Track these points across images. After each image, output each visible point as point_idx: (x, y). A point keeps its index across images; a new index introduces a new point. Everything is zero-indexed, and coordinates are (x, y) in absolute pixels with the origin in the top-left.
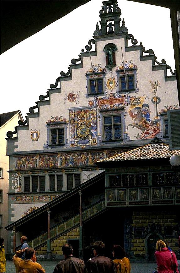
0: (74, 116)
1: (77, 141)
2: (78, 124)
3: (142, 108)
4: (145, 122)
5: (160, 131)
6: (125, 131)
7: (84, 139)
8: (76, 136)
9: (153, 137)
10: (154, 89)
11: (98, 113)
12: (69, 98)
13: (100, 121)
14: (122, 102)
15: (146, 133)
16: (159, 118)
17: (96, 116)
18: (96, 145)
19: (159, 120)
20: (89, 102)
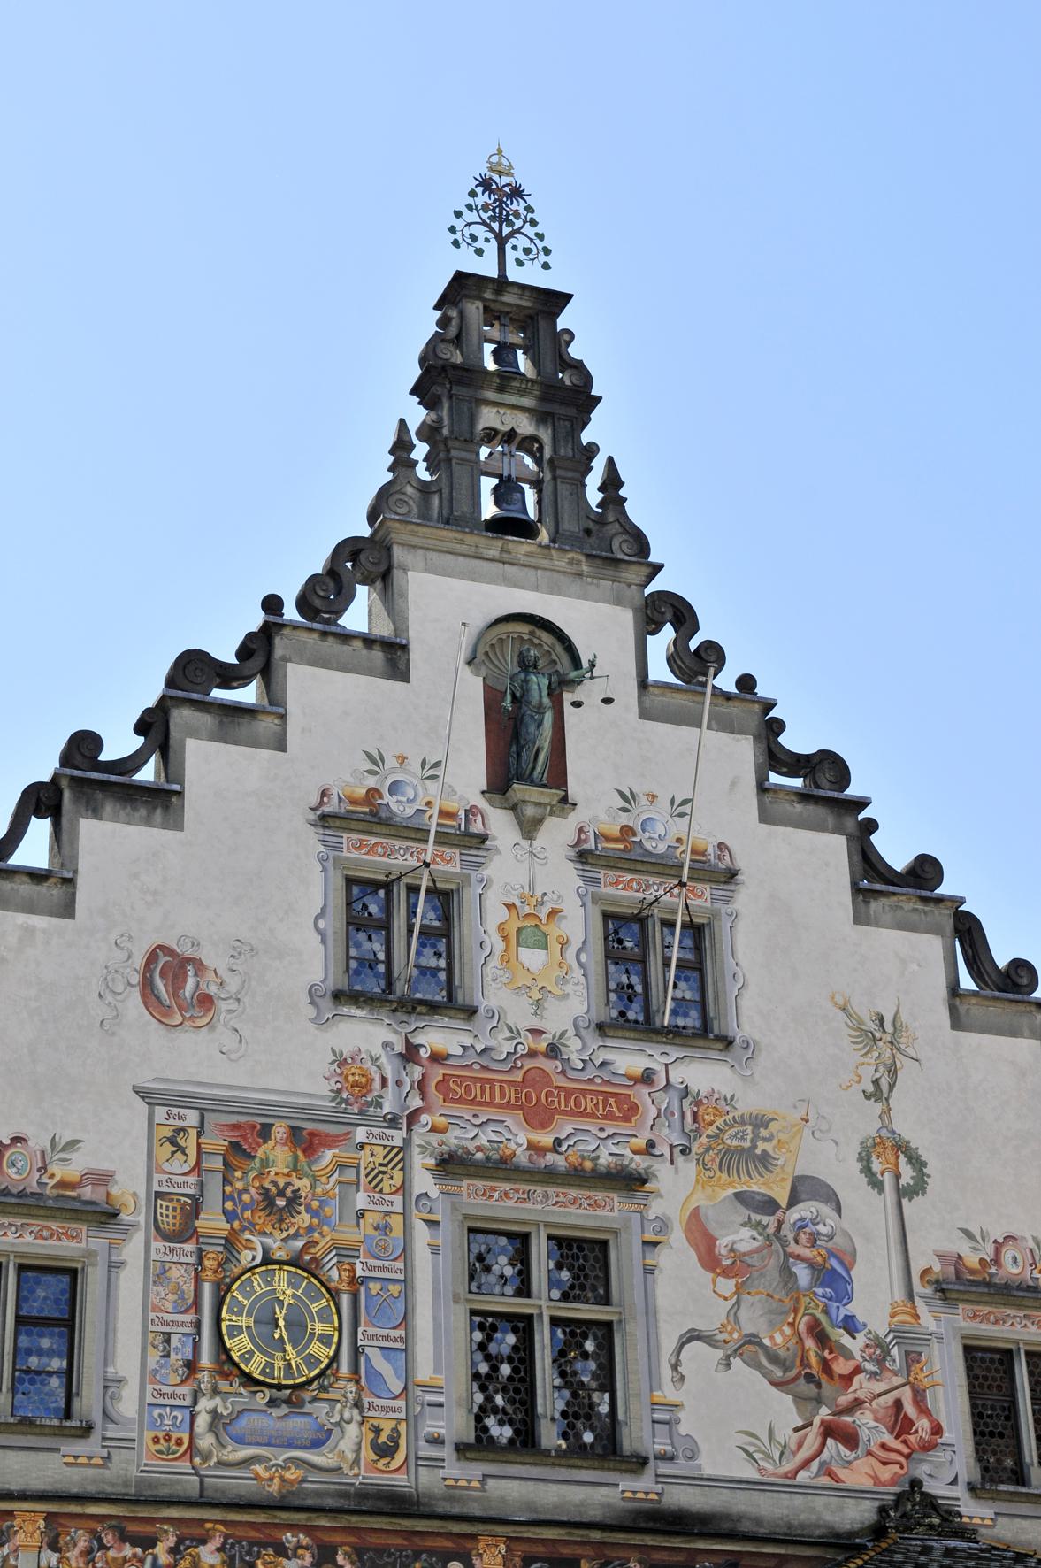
0: (193, 1159)
1: (214, 1413)
2: (231, 1244)
3: (793, 1201)
4: (822, 1338)
5: (937, 1430)
6: (653, 1381)
7: (290, 1395)
8: (206, 1359)
9: (886, 1473)
10: (868, 1073)
11: (424, 1181)
12: (147, 987)
13: (435, 1250)
14: (627, 1119)
15: (829, 1431)
16: (928, 1322)
17: (398, 1199)
18: (401, 1480)
19: (926, 1337)
20: (342, 1063)
